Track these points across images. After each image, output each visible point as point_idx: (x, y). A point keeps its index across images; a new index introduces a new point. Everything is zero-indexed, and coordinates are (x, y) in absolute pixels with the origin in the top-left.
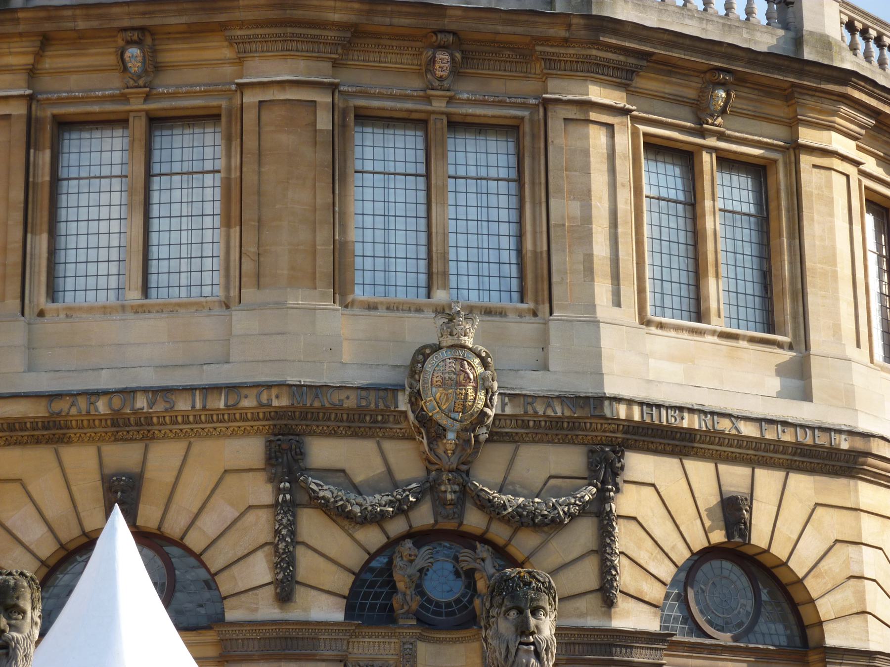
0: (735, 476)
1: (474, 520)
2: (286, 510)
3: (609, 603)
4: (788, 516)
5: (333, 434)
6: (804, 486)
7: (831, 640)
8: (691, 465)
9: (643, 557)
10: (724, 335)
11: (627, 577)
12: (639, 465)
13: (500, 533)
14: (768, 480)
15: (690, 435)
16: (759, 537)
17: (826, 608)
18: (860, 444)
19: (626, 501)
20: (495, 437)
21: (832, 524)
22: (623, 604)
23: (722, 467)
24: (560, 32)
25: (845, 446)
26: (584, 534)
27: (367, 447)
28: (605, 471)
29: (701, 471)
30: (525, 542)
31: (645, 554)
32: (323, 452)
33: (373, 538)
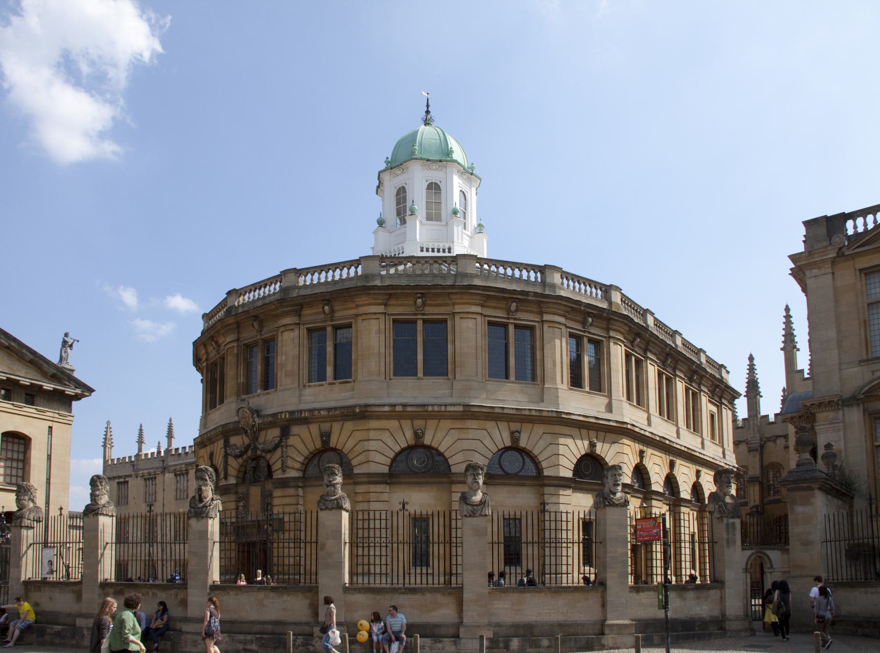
0: (325, 426)
1: (259, 453)
2: (226, 455)
3: (284, 471)
4: (344, 437)
5: (234, 435)
6: (349, 425)
7: (355, 472)
8: (311, 426)
9: (295, 456)
10: (330, 384)
11: (290, 463)
12: (295, 429)
13: (264, 454)
14: (336, 427)
15: (306, 419)
16: (333, 444)
17: (354, 462)
18: (363, 409)
19: (292, 440)
20: (260, 430)
21: (358, 436)
22: (288, 470)
23: (322, 425)
24: (273, 307)
25: (358, 410)
26: (279, 451)
27: (239, 437)
28: (285, 432)
29: (314, 428)
30: (269, 456)
31: (295, 455)
32: (234, 440)
33: (240, 460)
